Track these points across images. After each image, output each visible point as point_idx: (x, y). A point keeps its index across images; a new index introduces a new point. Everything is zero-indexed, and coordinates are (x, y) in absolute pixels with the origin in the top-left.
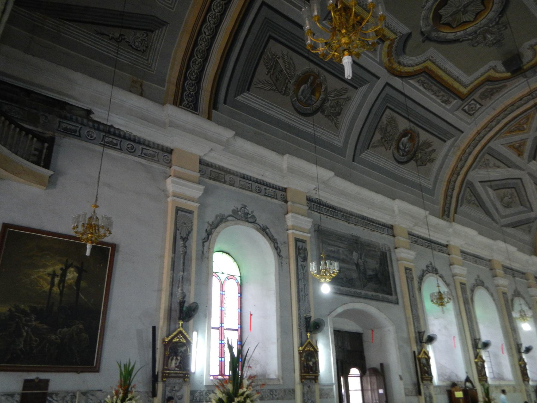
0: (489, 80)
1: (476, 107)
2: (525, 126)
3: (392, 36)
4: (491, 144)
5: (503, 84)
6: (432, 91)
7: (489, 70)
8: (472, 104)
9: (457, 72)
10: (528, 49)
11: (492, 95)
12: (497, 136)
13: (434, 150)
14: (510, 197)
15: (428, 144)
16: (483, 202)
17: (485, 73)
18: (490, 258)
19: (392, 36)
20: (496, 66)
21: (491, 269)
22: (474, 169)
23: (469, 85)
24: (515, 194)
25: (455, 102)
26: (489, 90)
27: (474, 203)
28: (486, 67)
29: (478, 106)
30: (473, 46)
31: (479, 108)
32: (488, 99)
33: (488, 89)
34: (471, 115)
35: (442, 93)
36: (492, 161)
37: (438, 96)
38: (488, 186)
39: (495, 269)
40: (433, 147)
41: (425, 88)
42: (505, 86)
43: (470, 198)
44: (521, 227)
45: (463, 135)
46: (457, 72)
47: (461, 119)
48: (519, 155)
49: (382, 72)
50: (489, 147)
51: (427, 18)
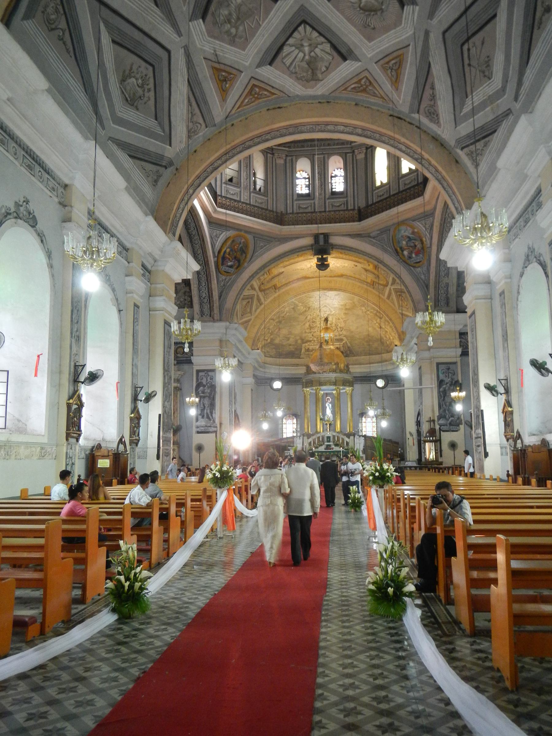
14: (140, 81)
16: (83, 52)
18: (67, 181)
21: (63, 205)
24: (151, 86)
27: (61, 39)
39: (71, 206)
43: (53, 17)
44: (143, 163)
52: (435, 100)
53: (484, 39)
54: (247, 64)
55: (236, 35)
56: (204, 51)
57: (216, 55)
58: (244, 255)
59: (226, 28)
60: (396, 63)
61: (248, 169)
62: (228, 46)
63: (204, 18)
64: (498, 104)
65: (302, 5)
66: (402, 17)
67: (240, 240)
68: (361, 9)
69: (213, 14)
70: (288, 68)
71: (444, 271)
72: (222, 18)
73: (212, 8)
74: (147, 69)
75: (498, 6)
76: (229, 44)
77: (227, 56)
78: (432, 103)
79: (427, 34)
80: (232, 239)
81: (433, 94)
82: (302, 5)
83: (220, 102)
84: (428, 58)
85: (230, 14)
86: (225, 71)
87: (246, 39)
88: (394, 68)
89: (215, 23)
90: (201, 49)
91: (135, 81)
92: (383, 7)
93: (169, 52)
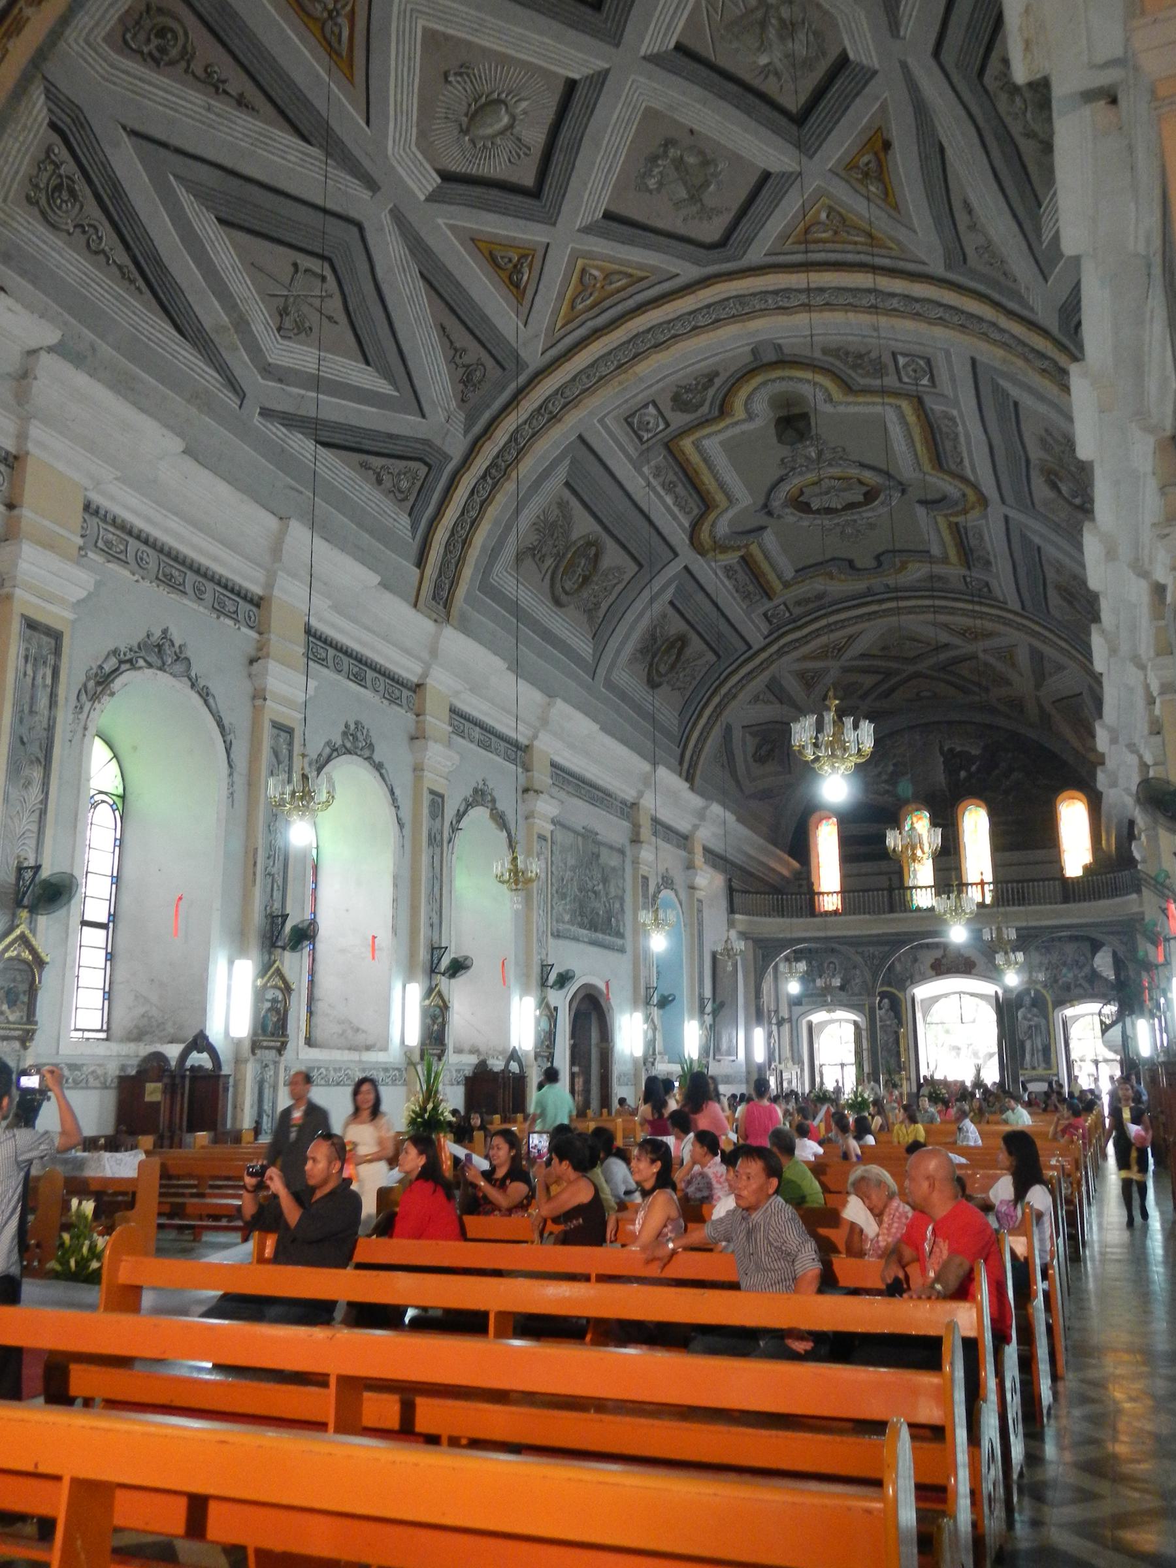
0: (848, 388)
1: (906, 366)
2: (823, 216)
3: (940, 519)
4: (939, 270)
5: (830, 359)
6: (955, 448)
7: (841, 403)
8: (909, 377)
9: (896, 431)
10: (757, 415)
11: (860, 356)
12: (911, 267)
13: (1046, 430)
15: (1043, 443)
17: (849, 404)
19: (940, 519)
20: (825, 401)
22: (1022, 301)
23: (891, 405)
25: (935, 407)
26: (860, 371)
28: (841, 409)
29: (902, 361)
30: (844, 450)
31: (905, 355)
32: (873, 355)
33: (862, 376)
34: (928, 362)
35: (944, 429)
36: (971, 242)
37: (957, 435)
38: (1041, 243)
40: (1044, 433)
41: (962, 461)
42: (825, 351)
45: (978, 357)
46: (896, 431)
47: (953, 379)
48: (887, 145)
49: (996, 510)
50: (949, 267)
51: (882, 503)
52: (203, 82)
53: (336, 322)
60: (340, 41)
64: (237, 349)
65: (617, 45)
66: (428, 160)
68: (499, 101)
75: (377, 371)
78: (198, 67)
79: (372, 185)
81: (225, 92)
82: (617, 45)
84: (321, 147)
88: (330, 23)
91: (1029, 115)
92: (467, 138)
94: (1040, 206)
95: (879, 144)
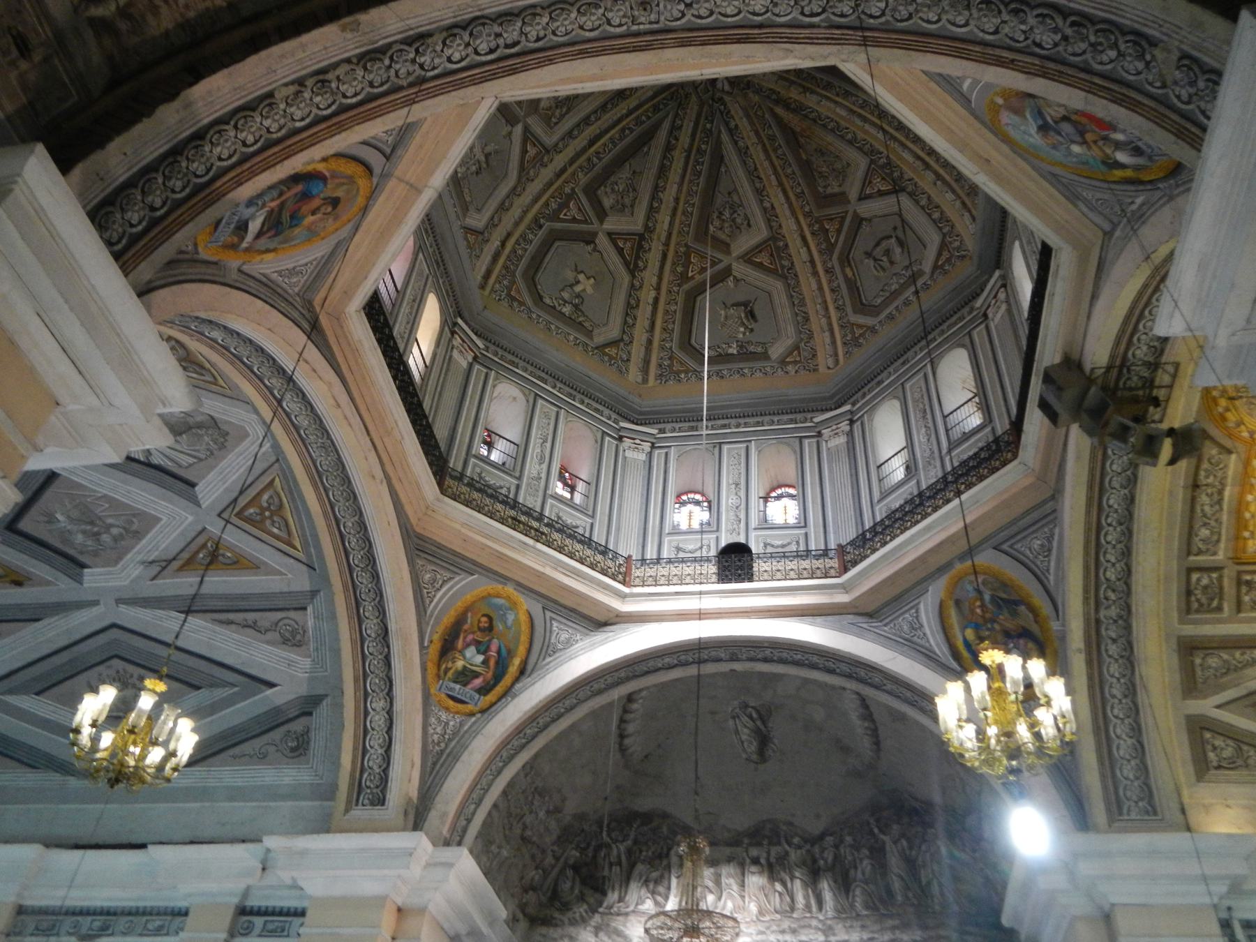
44: (231, 752)
48: (18, 584)
54: (190, 518)
55: (124, 528)
56: (138, 577)
57: (151, 563)
58: (1023, 608)
59: (108, 540)
61: (929, 416)
62: (144, 541)
63: (83, 566)
67: (970, 588)
69: (82, 553)
70: (200, 460)
71: (1121, 55)
72: (89, 543)
73: (71, 552)
74: (109, 667)
76: (140, 540)
77: (164, 545)
80: (951, 603)
83: (256, 575)
85: (84, 532)
86: (197, 552)
87: (134, 515)
89: (95, 554)
90: (132, 581)
93: (114, 626)
94: (38, 694)
95: (15, 578)
